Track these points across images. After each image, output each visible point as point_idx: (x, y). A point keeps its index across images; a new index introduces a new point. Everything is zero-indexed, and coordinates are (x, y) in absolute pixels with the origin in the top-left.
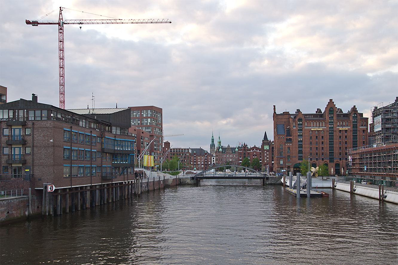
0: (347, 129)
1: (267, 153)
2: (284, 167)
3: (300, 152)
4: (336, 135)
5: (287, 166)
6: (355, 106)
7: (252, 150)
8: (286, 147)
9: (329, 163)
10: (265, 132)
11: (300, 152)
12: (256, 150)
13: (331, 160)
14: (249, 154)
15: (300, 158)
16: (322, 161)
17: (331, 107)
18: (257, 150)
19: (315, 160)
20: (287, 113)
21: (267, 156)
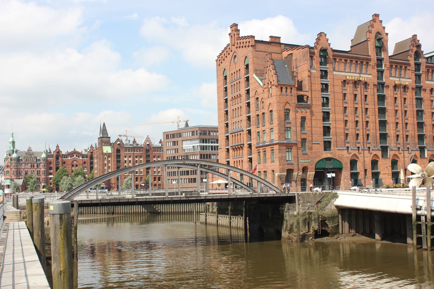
0: (407, 83)
1: (108, 159)
2: (295, 167)
3: (327, 130)
4: (388, 93)
5: (301, 167)
6: (415, 36)
7: (71, 157)
8: (299, 115)
9: (380, 157)
10: (104, 124)
11: (327, 130)
12: (76, 156)
13: (384, 149)
14: (64, 163)
15: (327, 145)
16: (369, 155)
17: (378, 30)
18: (79, 157)
19: (356, 152)
20: (277, 41)
21: (108, 165)
